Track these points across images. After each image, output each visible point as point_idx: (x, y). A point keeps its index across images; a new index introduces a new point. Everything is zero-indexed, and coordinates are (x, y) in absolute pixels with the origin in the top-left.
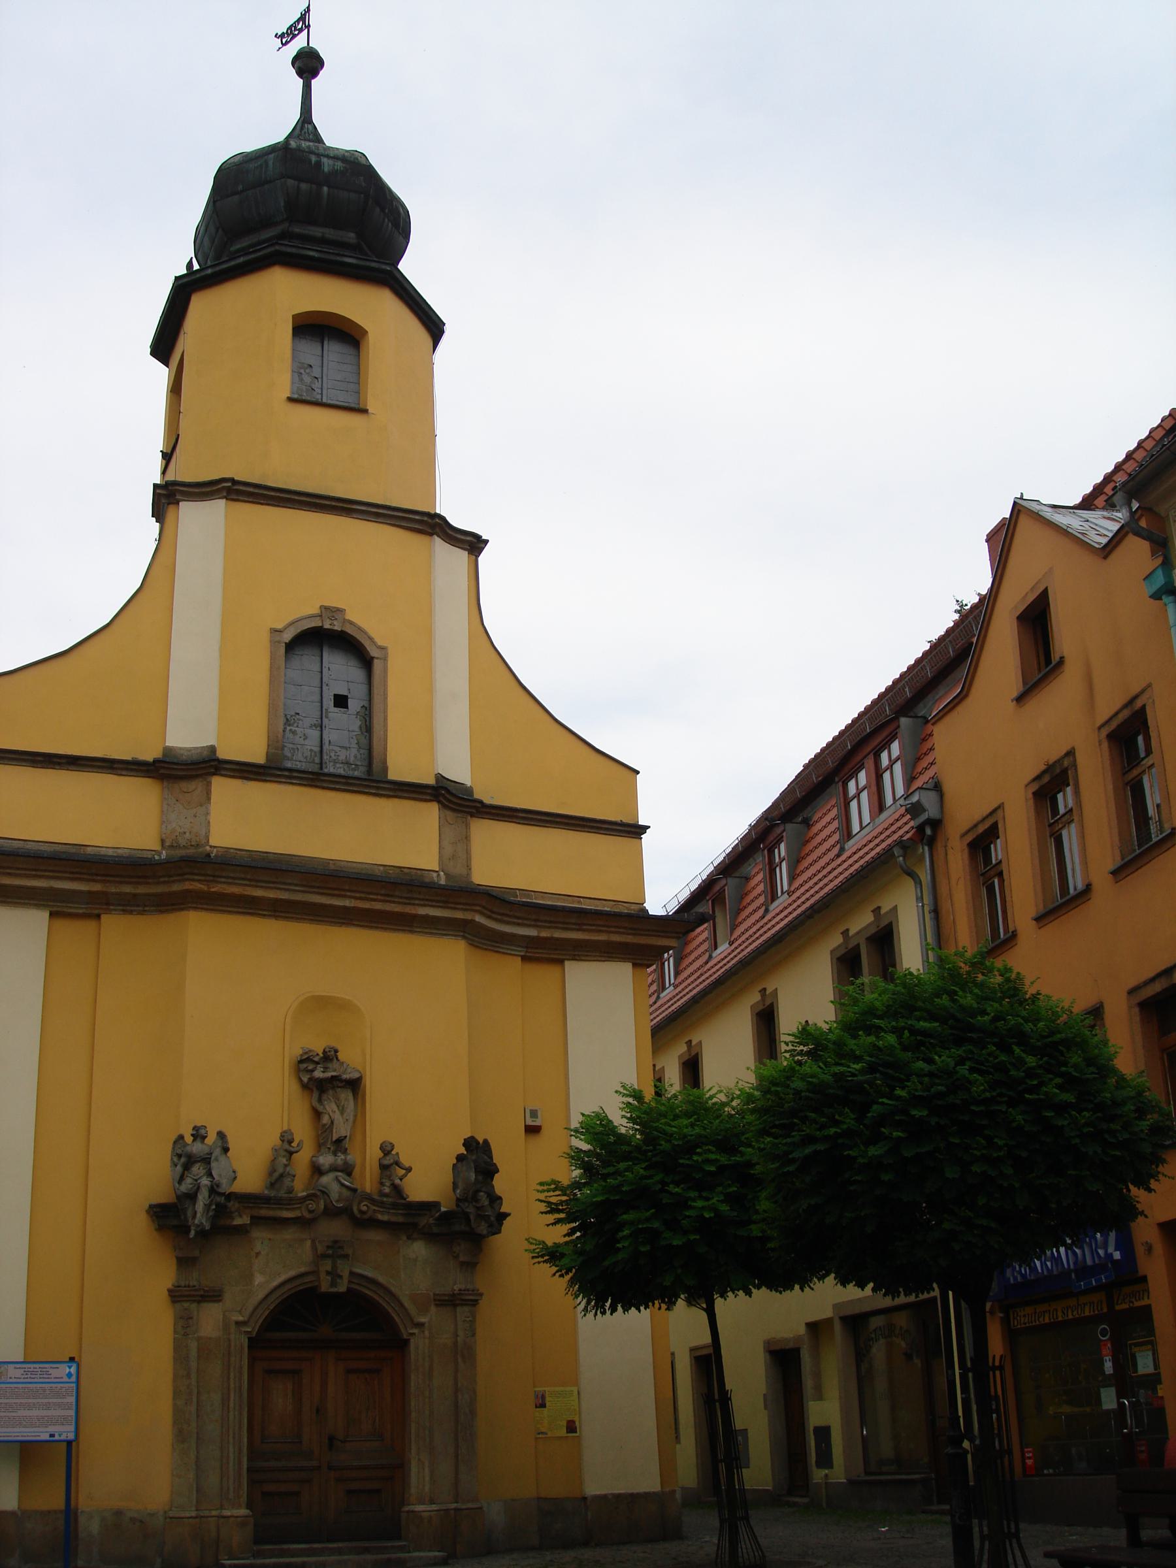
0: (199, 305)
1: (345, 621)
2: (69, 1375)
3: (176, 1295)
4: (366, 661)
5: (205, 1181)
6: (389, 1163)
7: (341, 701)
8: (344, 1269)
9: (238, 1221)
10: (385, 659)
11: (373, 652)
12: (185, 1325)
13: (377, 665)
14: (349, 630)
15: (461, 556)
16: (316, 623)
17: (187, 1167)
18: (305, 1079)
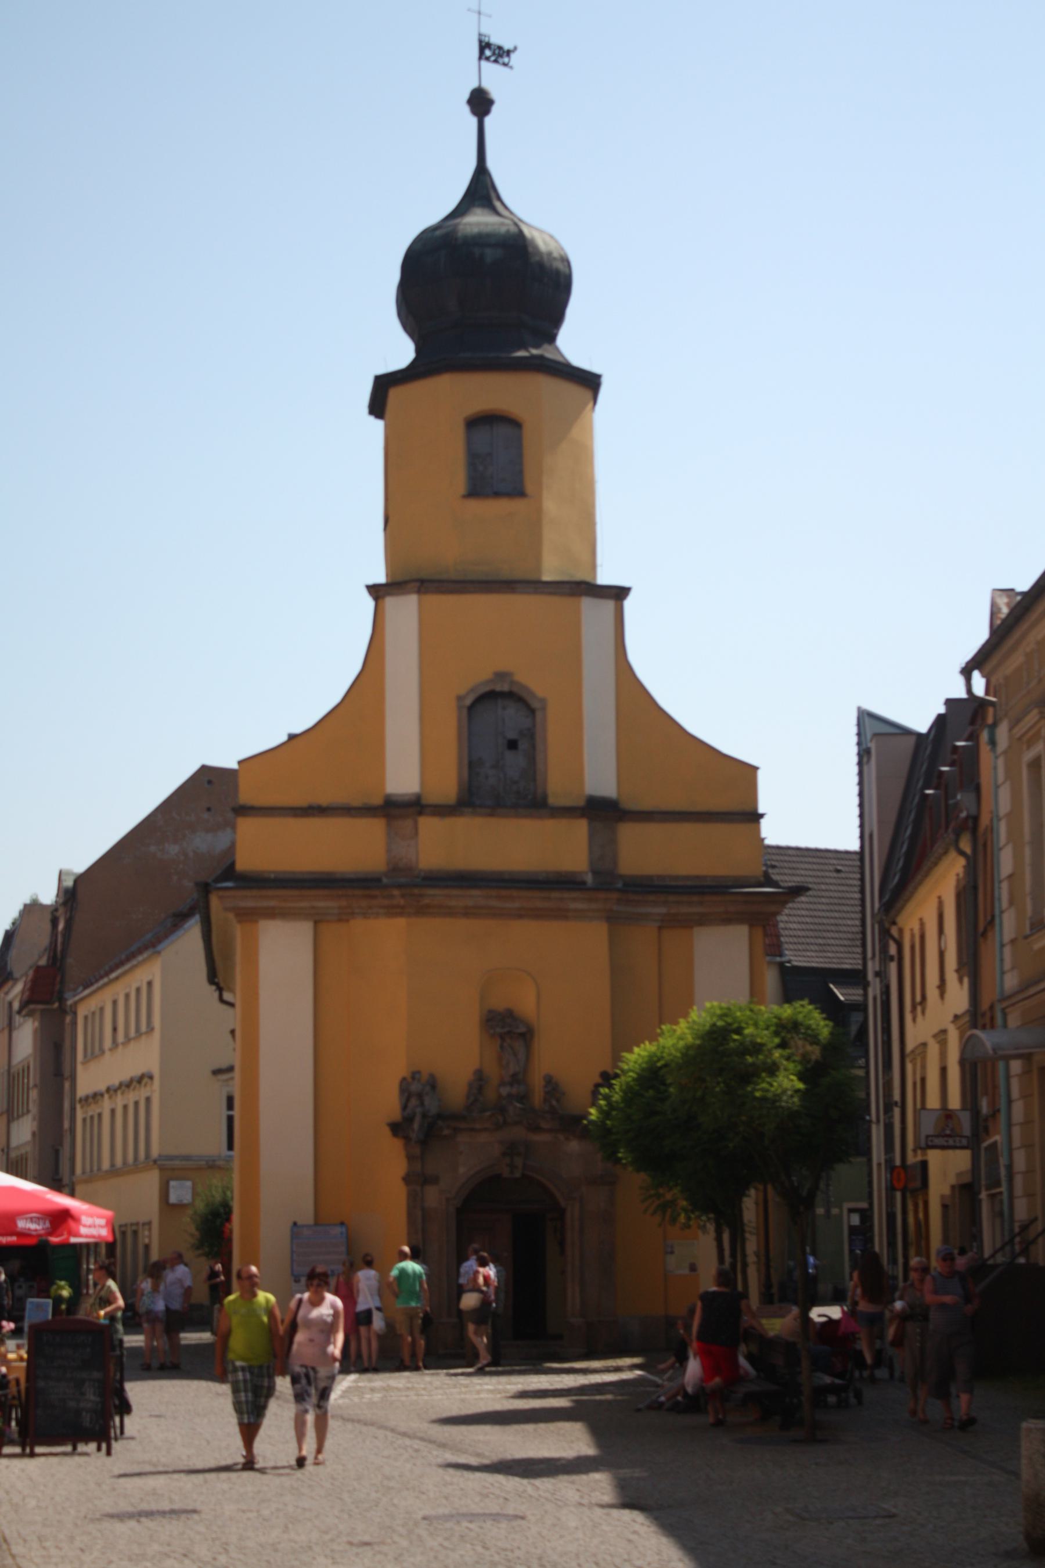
0: (395, 395)
1: (513, 683)
2: (342, 1233)
3: (407, 1179)
4: (532, 711)
5: (419, 1110)
6: (552, 1086)
7: (512, 745)
8: (519, 1161)
9: (446, 1132)
10: (544, 709)
11: (535, 704)
12: (415, 1200)
13: (539, 715)
14: (515, 689)
15: (610, 605)
16: (487, 689)
17: (408, 1100)
18: (492, 1031)
